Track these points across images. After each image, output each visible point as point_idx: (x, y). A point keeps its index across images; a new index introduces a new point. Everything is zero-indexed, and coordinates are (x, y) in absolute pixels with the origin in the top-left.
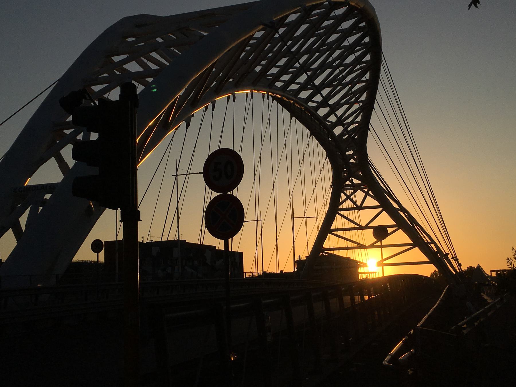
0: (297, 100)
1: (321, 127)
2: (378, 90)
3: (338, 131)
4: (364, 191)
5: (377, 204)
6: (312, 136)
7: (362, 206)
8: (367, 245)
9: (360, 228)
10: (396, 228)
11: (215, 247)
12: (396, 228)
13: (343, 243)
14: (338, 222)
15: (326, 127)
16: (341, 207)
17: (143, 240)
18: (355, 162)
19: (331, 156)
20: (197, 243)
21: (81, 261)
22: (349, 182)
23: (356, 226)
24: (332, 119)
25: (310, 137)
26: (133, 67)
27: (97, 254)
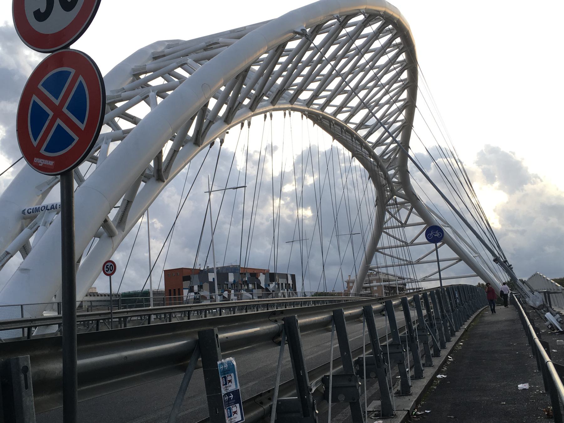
0: (336, 119)
2: (416, 107)
3: (378, 151)
4: (407, 209)
5: (420, 220)
6: (353, 158)
9: (407, 245)
13: (389, 261)
14: (384, 240)
15: (367, 148)
18: (397, 180)
19: (373, 176)
21: (148, 290)
22: (393, 201)
24: (373, 139)
25: (352, 159)
26: (159, 82)
27: (109, 277)
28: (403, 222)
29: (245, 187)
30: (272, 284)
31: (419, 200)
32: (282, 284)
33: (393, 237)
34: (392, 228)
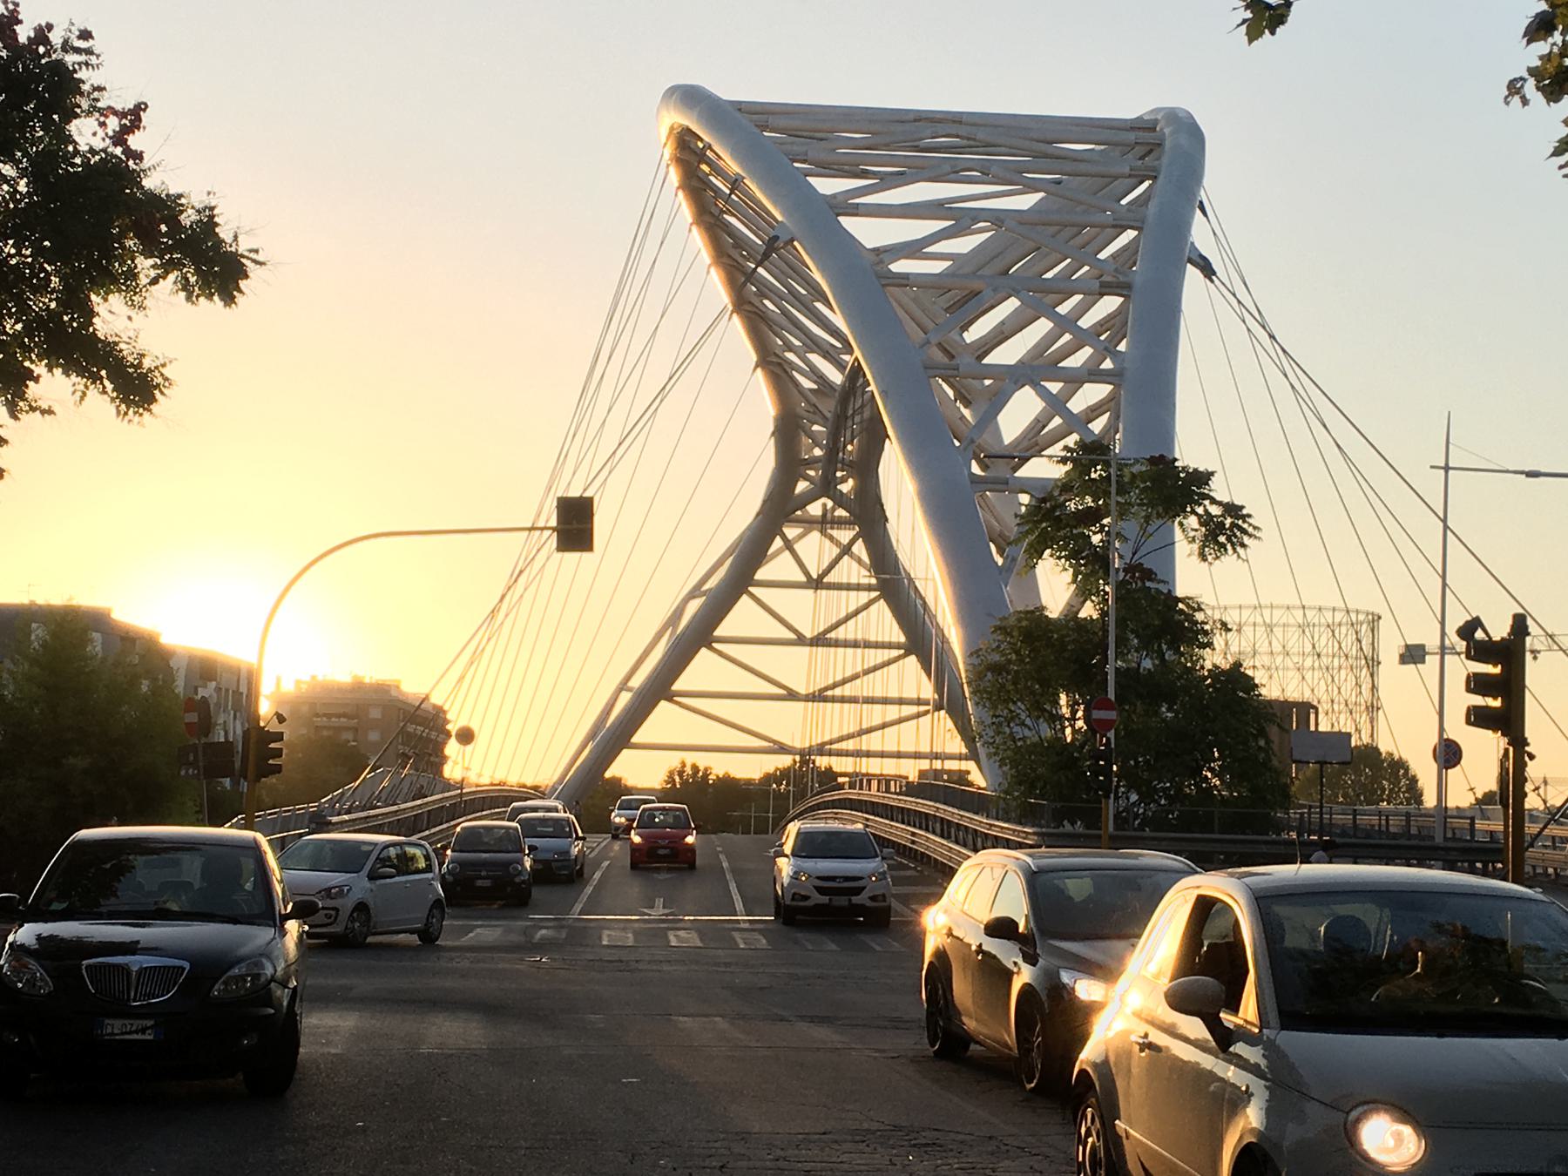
8: (803, 691)
9: (800, 640)
10: (902, 652)
12: (902, 652)
14: (742, 618)
16: (760, 575)
23: (793, 636)
28: (815, 576)
30: (206, 687)
32: (227, 690)
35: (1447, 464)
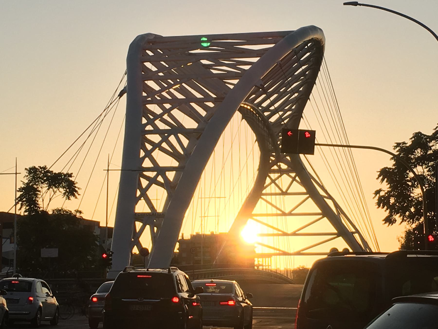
1: (257, 116)
5: (304, 190)
7: (288, 192)
9: (284, 214)
10: (321, 216)
11: (98, 223)
16: (264, 192)
17: (20, 213)
20: (90, 219)
23: (279, 212)
28: (284, 190)
29: (225, 197)
31: (305, 170)
33: (273, 205)
34: (271, 194)
35: (16, 175)
